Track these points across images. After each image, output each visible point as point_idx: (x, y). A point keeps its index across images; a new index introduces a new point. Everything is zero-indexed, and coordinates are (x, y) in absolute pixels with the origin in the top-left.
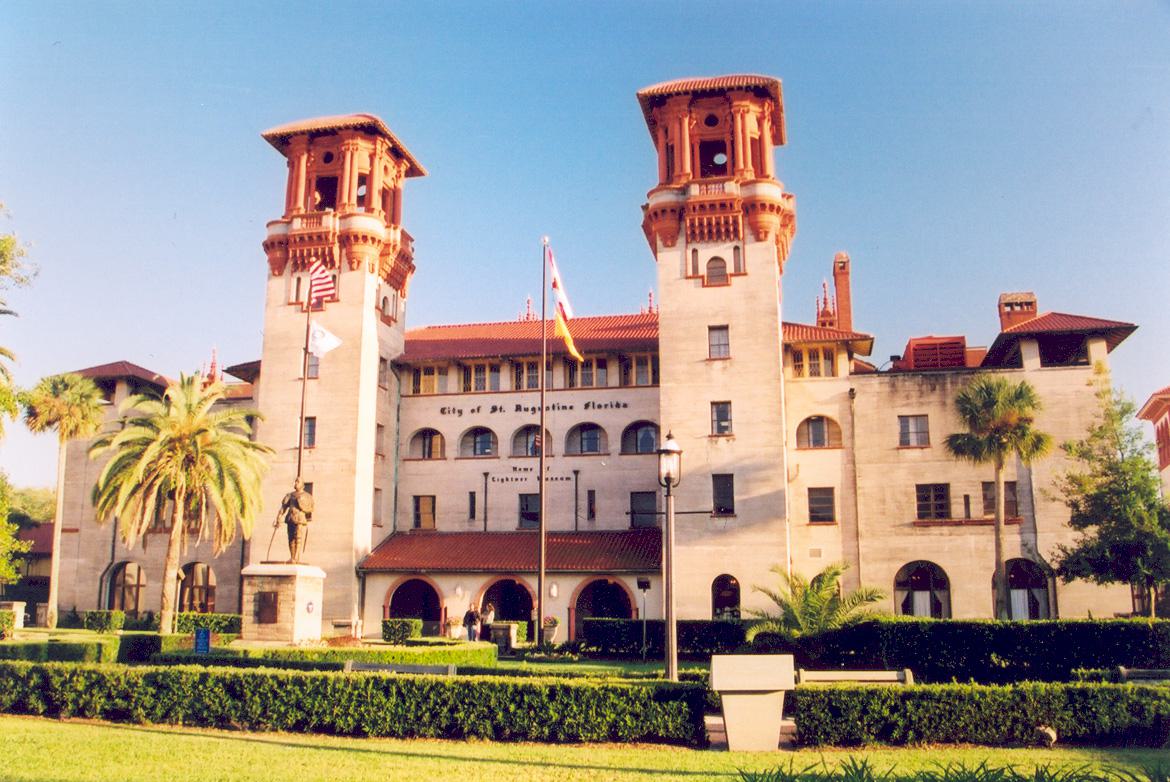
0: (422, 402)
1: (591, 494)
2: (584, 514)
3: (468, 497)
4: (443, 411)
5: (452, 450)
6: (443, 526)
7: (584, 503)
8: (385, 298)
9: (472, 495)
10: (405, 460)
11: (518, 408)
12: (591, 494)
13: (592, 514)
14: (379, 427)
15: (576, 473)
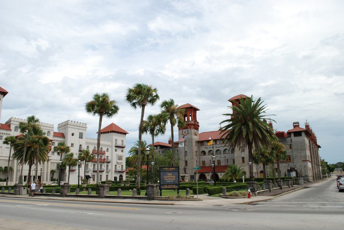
0: (202, 147)
1: (227, 160)
2: (226, 163)
3: (210, 161)
4: (205, 148)
5: (207, 154)
6: (206, 165)
7: (226, 161)
8: (195, 132)
9: (210, 160)
10: (201, 156)
11: (216, 147)
12: (227, 160)
13: (228, 162)
14: (196, 151)
15: (225, 156)
